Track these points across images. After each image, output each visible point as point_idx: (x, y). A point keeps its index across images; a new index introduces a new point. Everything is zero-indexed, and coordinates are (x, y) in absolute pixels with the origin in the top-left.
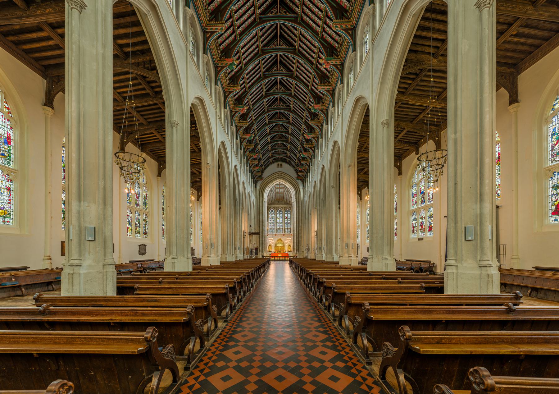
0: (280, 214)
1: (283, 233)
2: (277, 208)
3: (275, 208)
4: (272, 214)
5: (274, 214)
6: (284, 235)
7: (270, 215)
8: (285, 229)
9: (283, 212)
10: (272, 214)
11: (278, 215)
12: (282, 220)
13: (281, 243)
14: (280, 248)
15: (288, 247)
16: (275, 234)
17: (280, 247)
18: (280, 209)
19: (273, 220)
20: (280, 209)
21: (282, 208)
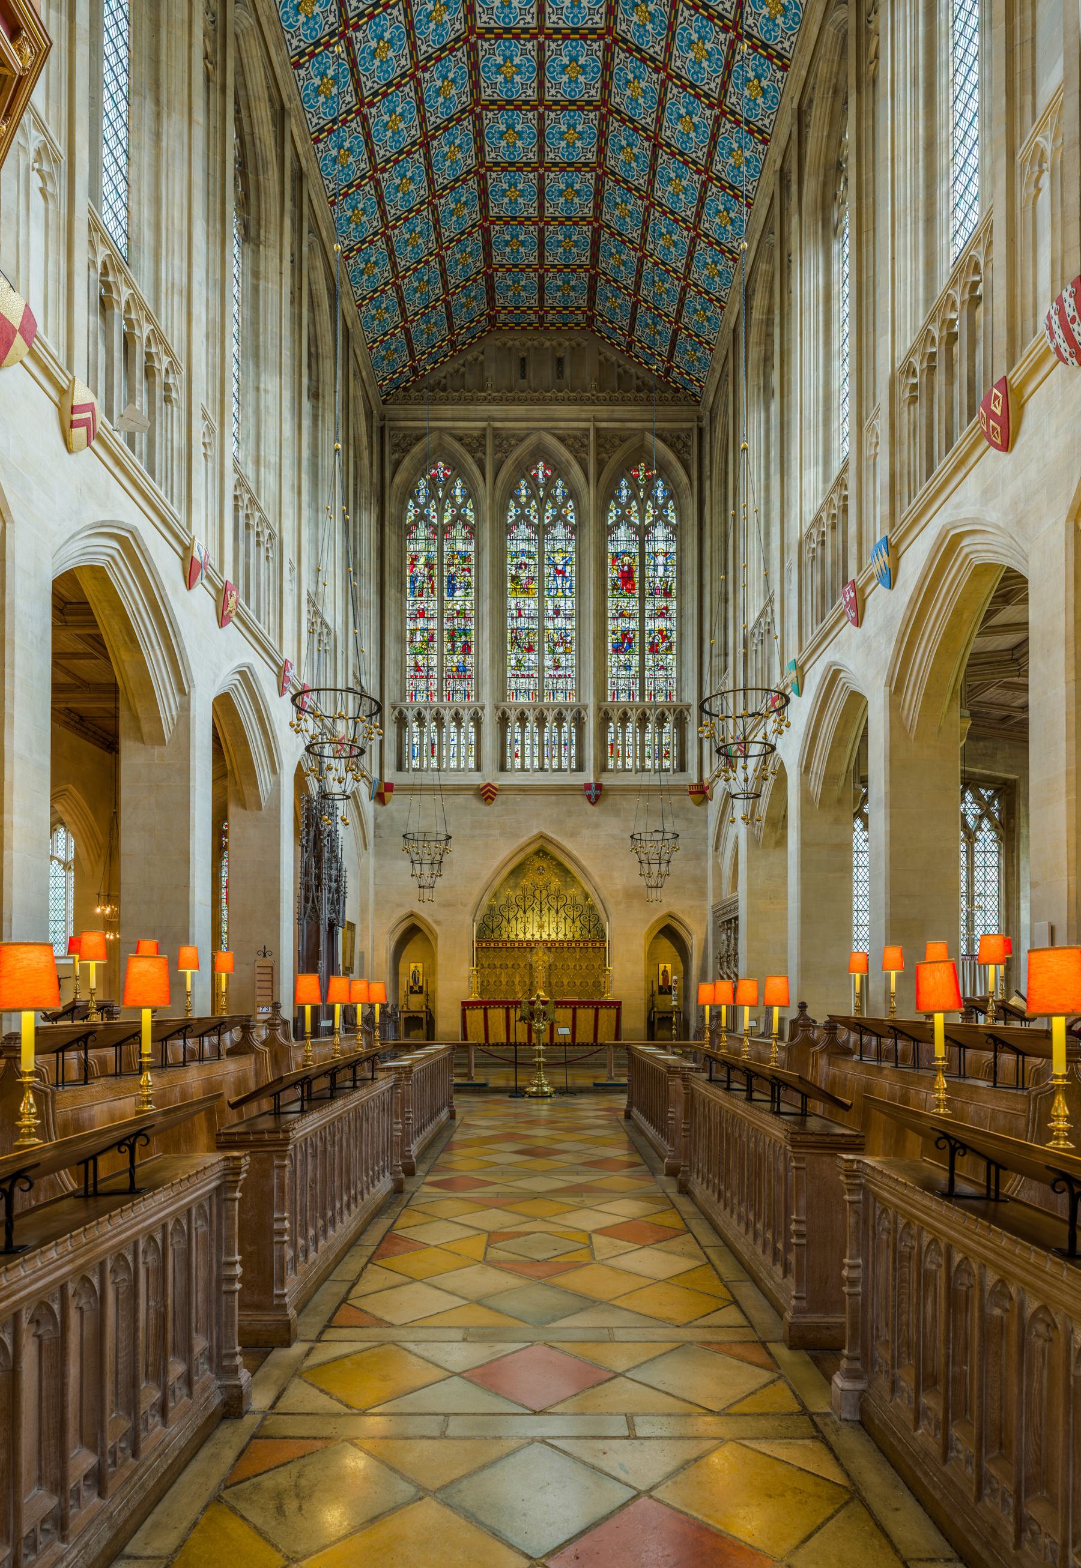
0: (542, 531)
1: (589, 776)
2: (504, 442)
3: (475, 444)
4: (442, 532)
5: (473, 531)
6: (596, 794)
7: (420, 544)
8: (604, 719)
9: (589, 498)
10: (442, 532)
11: (521, 540)
12: (568, 605)
13: (555, 902)
14: (541, 959)
15: (652, 957)
16: (477, 779)
17: (551, 946)
18: (541, 472)
19: (460, 600)
20: (541, 472)
21: (574, 443)
